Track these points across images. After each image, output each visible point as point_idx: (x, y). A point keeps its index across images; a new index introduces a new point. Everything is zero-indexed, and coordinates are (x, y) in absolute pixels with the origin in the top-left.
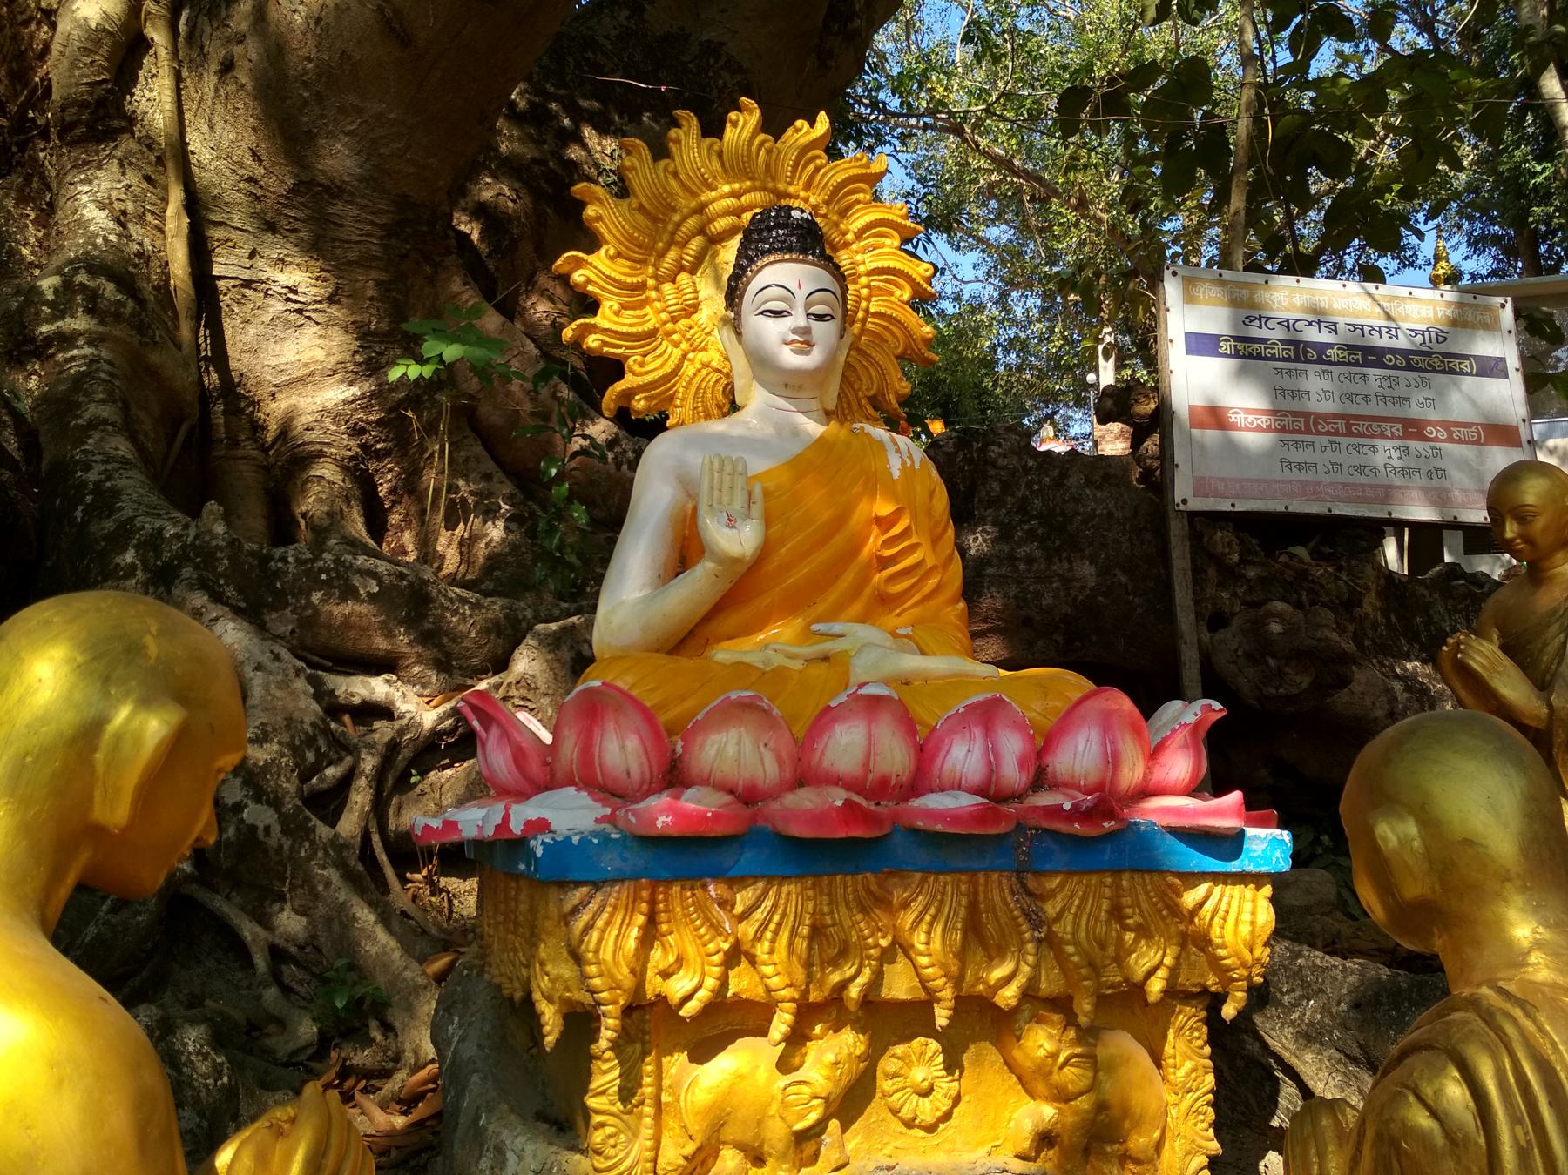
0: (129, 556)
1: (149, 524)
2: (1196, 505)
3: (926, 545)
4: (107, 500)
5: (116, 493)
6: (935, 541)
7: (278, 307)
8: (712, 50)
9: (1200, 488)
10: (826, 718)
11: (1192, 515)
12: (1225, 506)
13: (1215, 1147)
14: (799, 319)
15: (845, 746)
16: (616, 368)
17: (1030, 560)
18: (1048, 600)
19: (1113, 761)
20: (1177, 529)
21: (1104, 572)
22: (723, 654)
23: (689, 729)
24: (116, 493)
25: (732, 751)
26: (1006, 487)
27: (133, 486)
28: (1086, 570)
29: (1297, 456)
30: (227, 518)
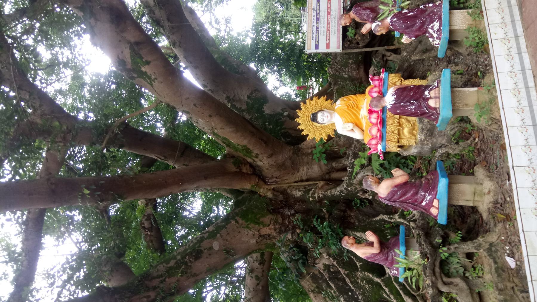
0: (349, 188)
1: (345, 186)
2: (341, 48)
3: (350, 102)
4: (341, 191)
5: (340, 190)
6: (350, 100)
7: (310, 171)
8: (249, 97)
9: (338, 48)
10: (371, 122)
11: (343, 49)
12: (341, 44)
13: (418, 79)
14: (325, 117)
15: (374, 121)
16: (329, 136)
17: (348, 69)
18: (355, 67)
19: (376, 92)
20: (344, 51)
21: (350, 59)
22: (364, 129)
23: (372, 136)
24: (340, 190)
25: (374, 131)
26: (337, 71)
27: (339, 189)
28: (350, 61)
29: (333, 32)
30: (344, 177)
